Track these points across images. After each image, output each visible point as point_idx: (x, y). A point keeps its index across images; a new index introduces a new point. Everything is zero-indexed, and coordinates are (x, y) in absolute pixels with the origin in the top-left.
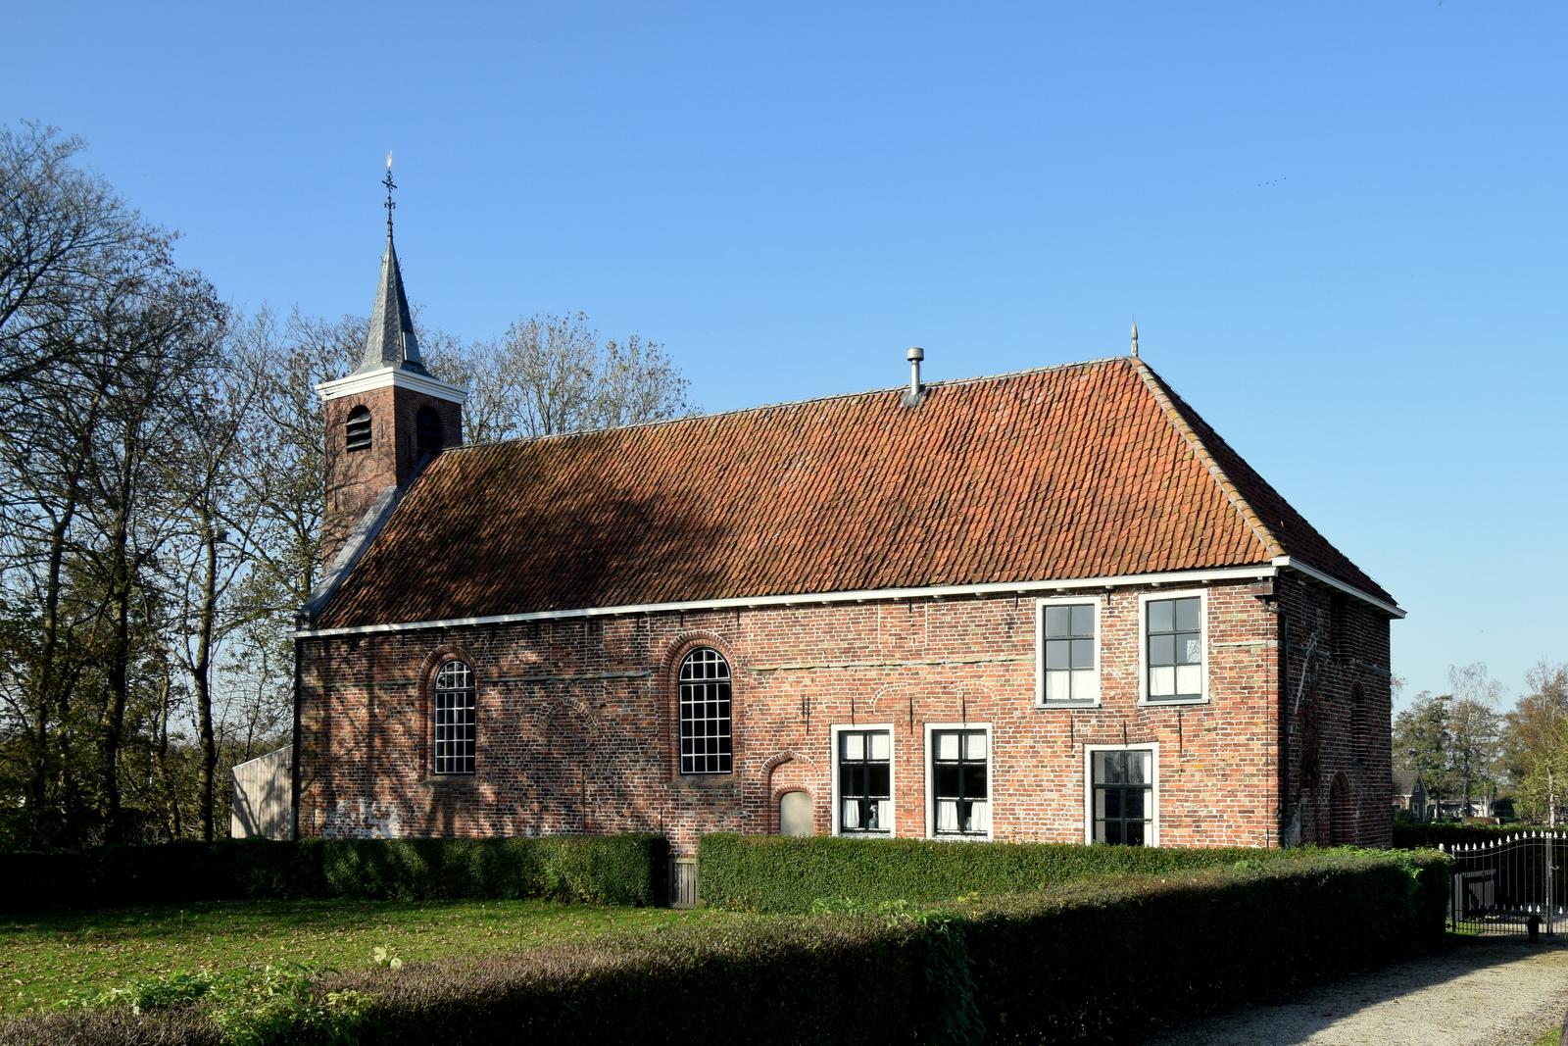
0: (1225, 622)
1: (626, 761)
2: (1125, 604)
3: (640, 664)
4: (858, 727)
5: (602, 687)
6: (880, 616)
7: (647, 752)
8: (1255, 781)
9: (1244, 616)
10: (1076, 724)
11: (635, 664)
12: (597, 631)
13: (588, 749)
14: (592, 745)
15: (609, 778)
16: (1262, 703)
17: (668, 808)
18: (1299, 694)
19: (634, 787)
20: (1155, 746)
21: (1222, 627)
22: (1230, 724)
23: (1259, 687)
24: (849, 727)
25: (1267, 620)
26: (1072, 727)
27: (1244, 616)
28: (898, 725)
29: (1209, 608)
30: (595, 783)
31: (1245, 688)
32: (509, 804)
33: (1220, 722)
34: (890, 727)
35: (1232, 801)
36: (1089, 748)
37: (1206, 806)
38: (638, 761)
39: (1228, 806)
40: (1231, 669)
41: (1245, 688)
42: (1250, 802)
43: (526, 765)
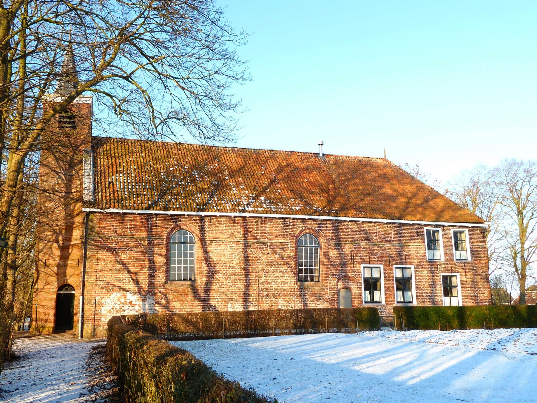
1: (278, 276)
2: (448, 231)
3: (285, 238)
5: (267, 246)
6: (377, 228)
7: (288, 273)
9: (478, 237)
11: (282, 238)
12: (265, 223)
13: (260, 271)
14: (262, 269)
15: (270, 283)
16: (484, 262)
17: (297, 295)
19: (282, 287)
20: (458, 274)
21: (473, 240)
24: (368, 265)
27: (478, 237)
28: (385, 265)
30: (263, 285)
32: (219, 294)
34: (382, 266)
38: (284, 276)
40: (476, 252)
43: (229, 277)
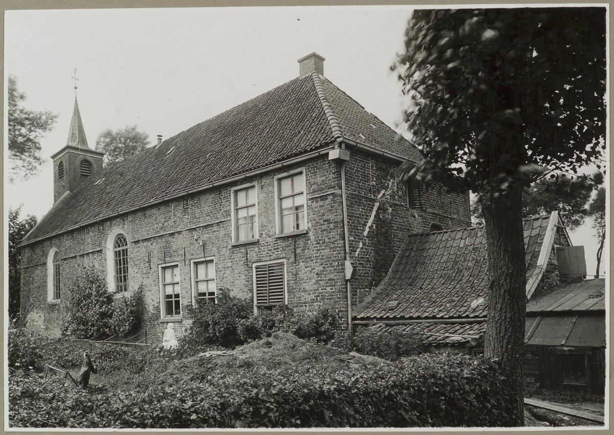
0: (314, 184)
4: (168, 265)
8: (332, 276)
10: (248, 252)
18: (369, 224)
22: (319, 243)
23: (333, 220)
25: (335, 178)
26: (247, 254)
29: (306, 178)
31: (325, 221)
33: (314, 243)
35: (322, 289)
36: (254, 265)
37: (309, 294)
39: (320, 293)
41: (325, 221)
42: (332, 289)
